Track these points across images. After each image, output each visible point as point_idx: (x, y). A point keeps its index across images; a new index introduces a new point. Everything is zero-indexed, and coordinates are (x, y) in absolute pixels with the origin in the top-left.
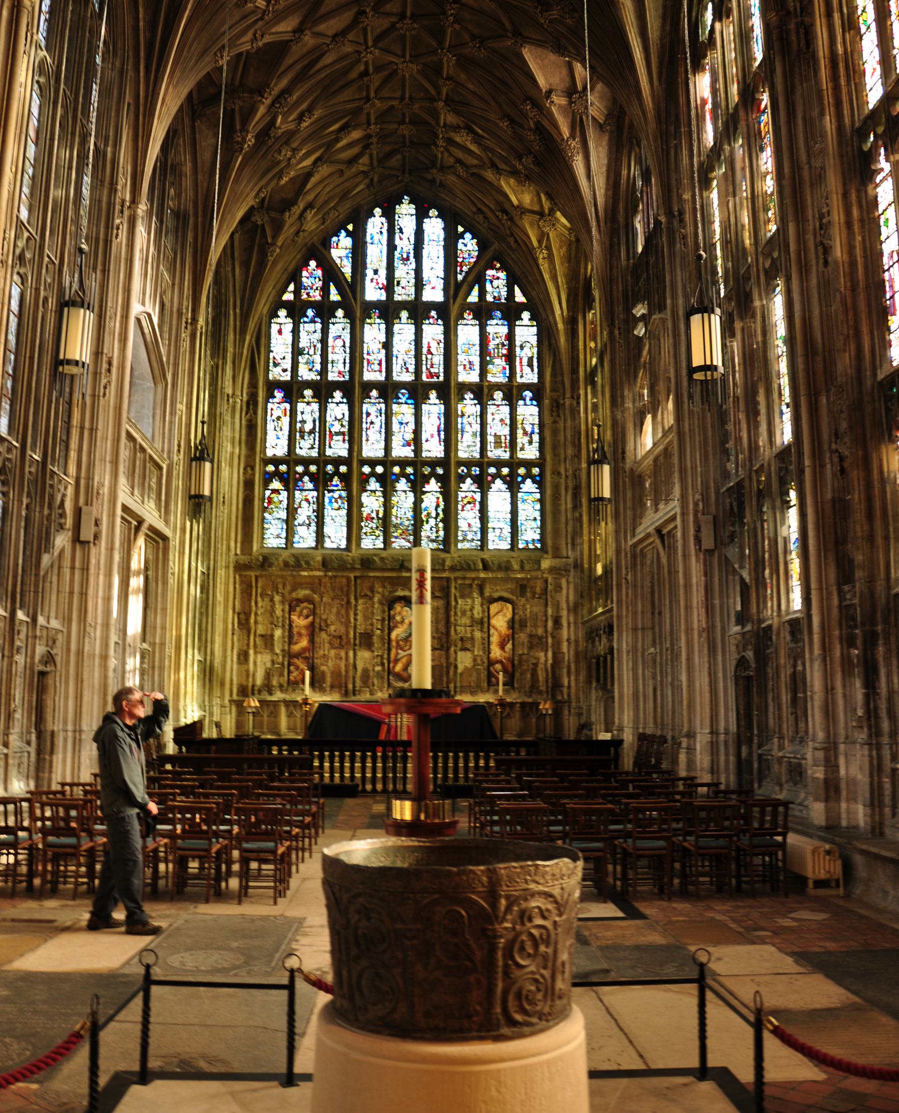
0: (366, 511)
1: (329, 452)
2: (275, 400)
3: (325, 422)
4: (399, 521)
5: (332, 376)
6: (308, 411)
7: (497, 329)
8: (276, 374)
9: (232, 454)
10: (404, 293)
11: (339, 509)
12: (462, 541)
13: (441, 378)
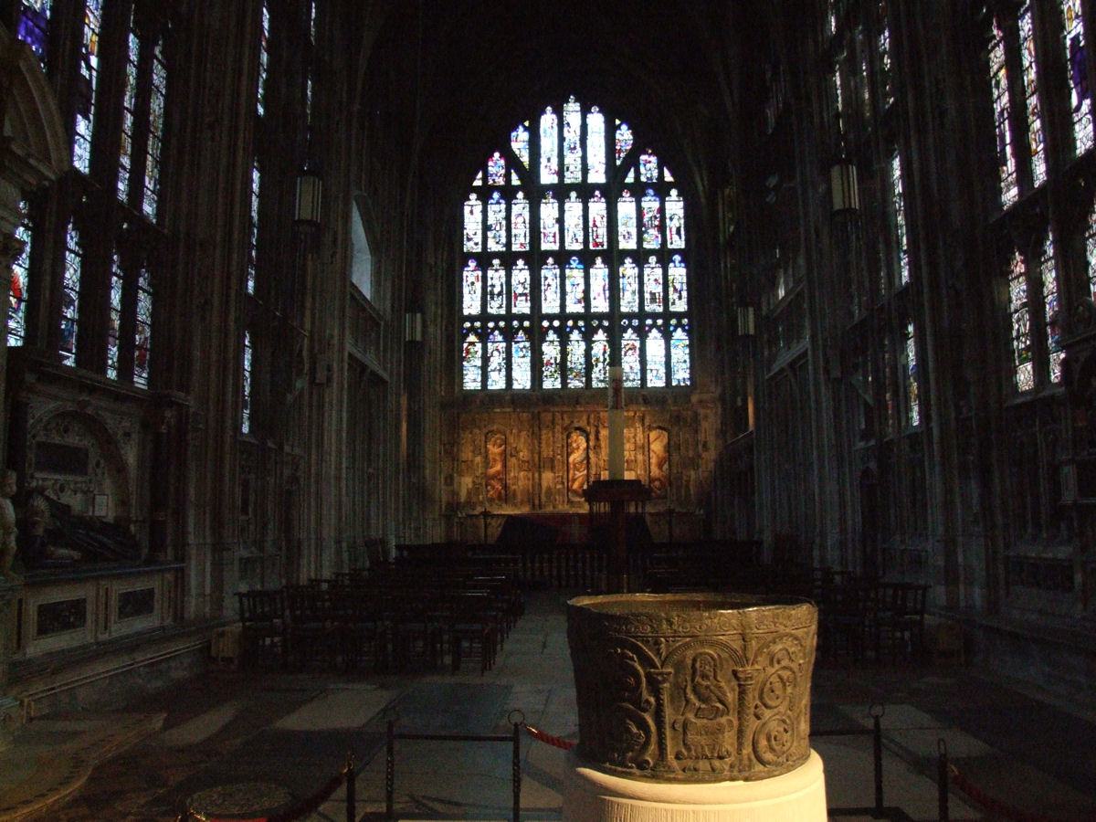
0: (546, 358)
1: (514, 310)
2: (469, 269)
3: (511, 285)
4: (573, 366)
5: (515, 248)
6: (497, 277)
7: (650, 204)
8: (469, 246)
9: (436, 313)
10: (573, 176)
11: (524, 356)
12: (626, 381)
13: (605, 247)
